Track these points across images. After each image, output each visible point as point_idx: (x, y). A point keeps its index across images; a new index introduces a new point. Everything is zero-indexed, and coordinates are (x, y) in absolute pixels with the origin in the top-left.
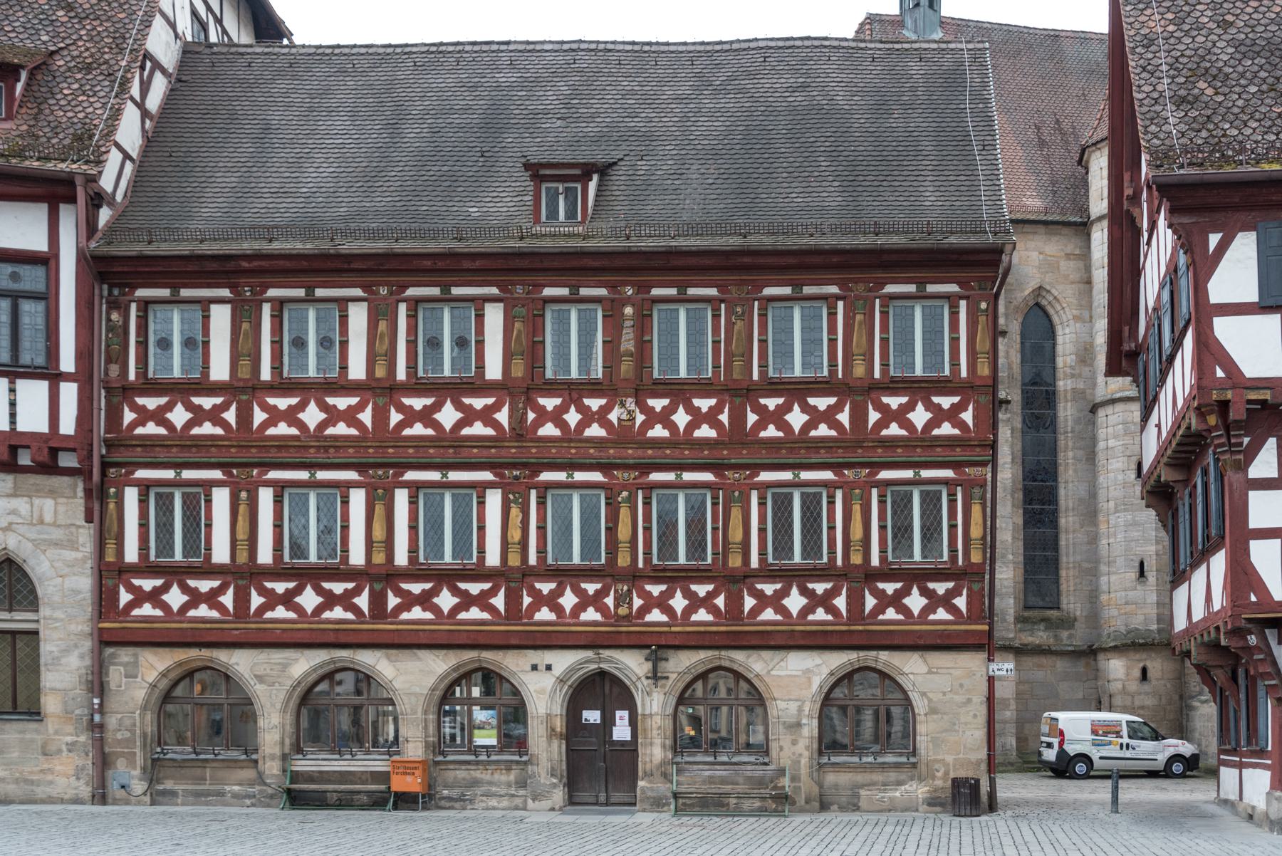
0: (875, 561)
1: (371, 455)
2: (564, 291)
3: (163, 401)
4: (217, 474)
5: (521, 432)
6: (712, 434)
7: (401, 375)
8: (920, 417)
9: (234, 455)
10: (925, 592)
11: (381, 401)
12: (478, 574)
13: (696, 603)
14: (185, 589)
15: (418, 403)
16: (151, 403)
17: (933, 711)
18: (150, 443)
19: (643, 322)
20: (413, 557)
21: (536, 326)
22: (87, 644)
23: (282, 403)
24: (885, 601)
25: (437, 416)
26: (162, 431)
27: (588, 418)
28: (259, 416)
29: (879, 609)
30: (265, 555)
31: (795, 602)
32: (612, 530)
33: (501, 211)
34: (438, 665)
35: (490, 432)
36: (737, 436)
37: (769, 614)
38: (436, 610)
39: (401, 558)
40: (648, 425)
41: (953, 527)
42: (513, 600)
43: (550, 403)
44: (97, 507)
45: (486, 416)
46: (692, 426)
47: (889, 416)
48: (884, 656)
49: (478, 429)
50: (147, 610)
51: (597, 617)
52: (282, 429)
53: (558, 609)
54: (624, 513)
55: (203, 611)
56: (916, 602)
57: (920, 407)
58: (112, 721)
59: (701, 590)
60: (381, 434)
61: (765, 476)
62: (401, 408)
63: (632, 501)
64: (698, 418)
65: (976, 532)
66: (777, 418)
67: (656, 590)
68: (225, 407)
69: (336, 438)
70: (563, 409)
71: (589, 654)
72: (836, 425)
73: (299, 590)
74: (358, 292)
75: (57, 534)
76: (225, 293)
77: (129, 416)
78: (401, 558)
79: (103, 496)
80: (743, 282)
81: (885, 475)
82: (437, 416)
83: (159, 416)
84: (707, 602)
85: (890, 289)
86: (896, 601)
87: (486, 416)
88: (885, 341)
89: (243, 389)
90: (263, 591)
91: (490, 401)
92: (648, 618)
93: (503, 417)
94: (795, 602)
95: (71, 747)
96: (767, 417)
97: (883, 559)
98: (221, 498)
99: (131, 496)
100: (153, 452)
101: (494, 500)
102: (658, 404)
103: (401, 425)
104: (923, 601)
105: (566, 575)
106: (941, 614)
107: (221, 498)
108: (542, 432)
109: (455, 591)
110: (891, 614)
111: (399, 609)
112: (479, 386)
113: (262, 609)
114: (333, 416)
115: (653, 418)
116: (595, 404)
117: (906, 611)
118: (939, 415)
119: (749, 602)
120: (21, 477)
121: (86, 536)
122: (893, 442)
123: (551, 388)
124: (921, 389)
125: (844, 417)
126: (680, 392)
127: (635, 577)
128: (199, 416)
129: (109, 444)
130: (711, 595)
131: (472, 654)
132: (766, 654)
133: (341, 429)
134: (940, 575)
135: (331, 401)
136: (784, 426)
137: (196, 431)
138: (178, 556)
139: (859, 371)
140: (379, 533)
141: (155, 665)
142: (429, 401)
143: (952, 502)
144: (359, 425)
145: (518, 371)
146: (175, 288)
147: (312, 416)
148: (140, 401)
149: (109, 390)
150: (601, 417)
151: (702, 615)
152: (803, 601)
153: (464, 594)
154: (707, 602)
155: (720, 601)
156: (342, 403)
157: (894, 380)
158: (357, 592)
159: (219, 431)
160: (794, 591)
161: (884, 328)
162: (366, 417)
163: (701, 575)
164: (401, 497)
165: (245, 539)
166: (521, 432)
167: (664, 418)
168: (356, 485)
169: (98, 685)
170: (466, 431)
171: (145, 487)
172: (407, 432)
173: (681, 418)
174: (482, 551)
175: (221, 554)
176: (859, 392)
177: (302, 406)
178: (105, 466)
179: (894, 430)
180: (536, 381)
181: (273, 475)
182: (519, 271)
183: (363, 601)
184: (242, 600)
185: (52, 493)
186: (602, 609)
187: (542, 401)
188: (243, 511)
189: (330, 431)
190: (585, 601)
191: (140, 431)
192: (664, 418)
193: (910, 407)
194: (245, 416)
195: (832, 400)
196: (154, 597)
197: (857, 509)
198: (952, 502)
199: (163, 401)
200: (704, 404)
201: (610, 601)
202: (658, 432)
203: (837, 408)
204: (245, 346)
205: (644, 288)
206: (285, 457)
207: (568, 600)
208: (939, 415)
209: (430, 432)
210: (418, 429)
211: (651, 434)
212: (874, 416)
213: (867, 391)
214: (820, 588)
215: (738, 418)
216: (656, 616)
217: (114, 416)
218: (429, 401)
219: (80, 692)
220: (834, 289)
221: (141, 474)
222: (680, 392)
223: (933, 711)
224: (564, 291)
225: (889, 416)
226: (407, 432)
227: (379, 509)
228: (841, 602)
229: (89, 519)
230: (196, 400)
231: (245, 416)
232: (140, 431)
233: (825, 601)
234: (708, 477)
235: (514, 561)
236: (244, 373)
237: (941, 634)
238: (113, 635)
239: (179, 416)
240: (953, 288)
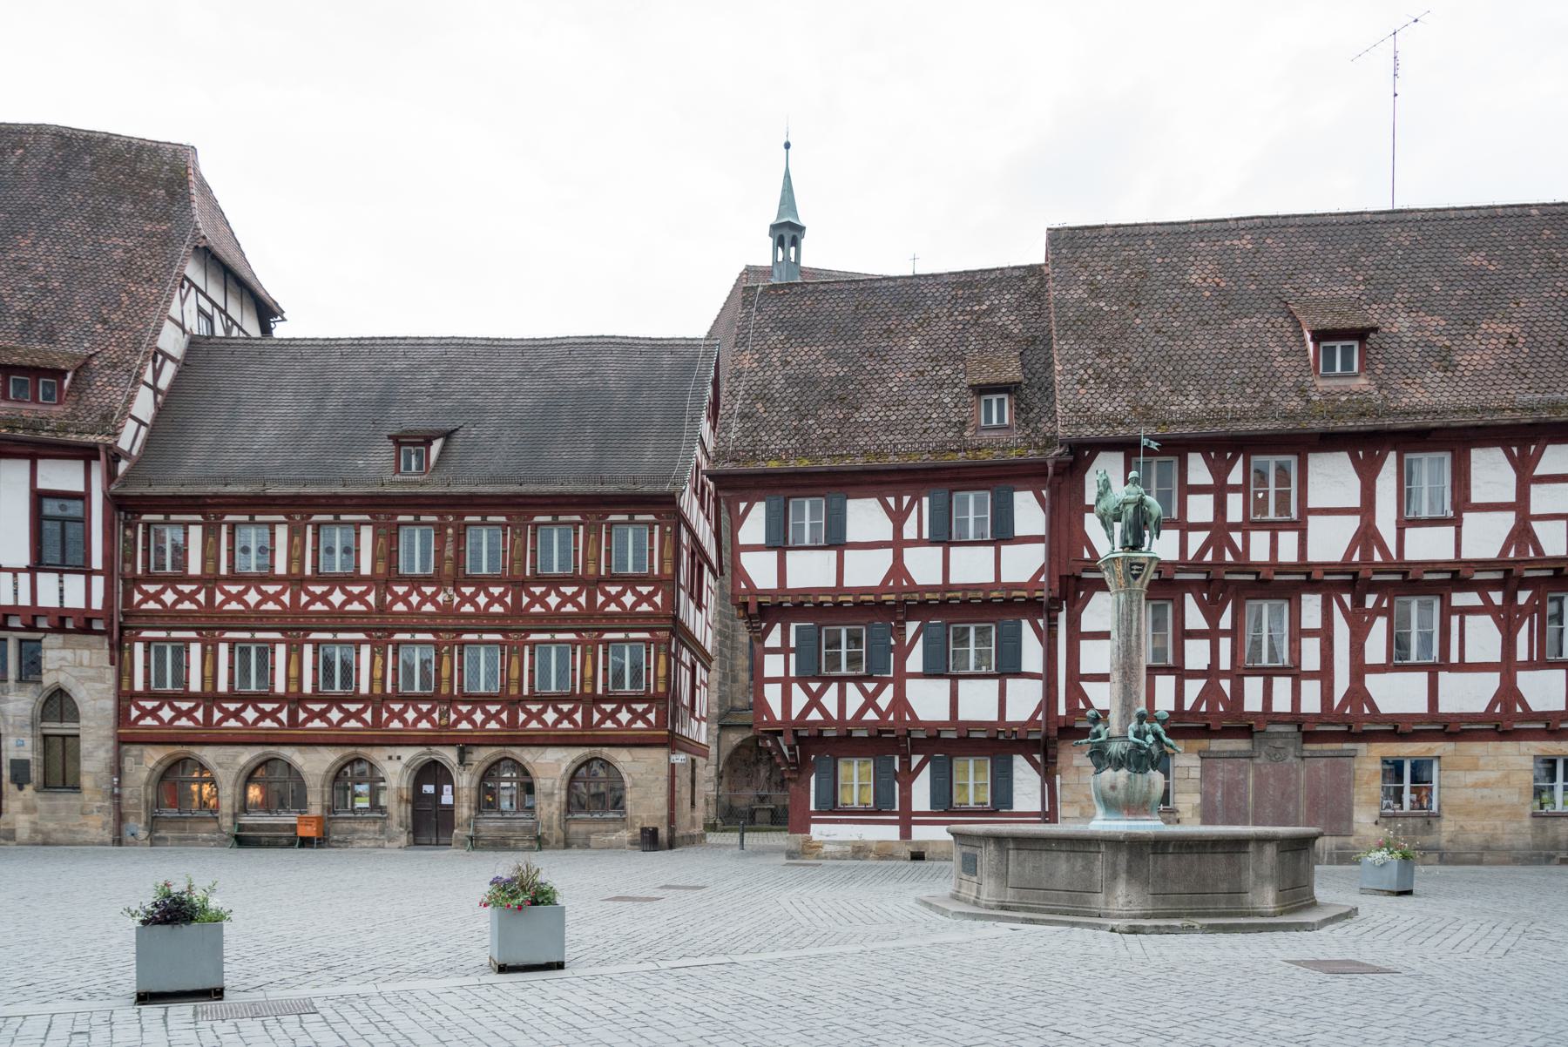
0: (600, 691)
1: (289, 623)
2: (410, 518)
3: (159, 587)
4: (193, 634)
5: (382, 608)
7: (308, 571)
8: (629, 599)
9: (204, 623)
10: (630, 710)
11: (295, 588)
13: (489, 717)
15: (318, 590)
16: (152, 589)
17: (635, 785)
18: (151, 614)
19: (460, 538)
21: (393, 540)
23: (234, 589)
25: (331, 598)
26: (158, 607)
27: (425, 599)
28: (219, 598)
31: (550, 716)
32: (438, 671)
33: (377, 468)
35: (363, 608)
36: (516, 611)
37: (534, 724)
40: (461, 604)
41: (648, 669)
43: (401, 590)
44: (117, 655)
45: (361, 598)
46: (488, 605)
47: (610, 599)
48: (605, 750)
49: (356, 606)
52: (234, 606)
54: (446, 660)
56: (624, 716)
57: (629, 593)
59: (493, 709)
60: (295, 609)
61: (534, 637)
62: (308, 593)
64: (492, 600)
65: (662, 672)
66: (541, 600)
67: (464, 709)
68: (198, 591)
69: (267, 612)
70: (409, 594)
72: (577, 604)
74: (282, 518)
75: (91, 673)
77: (137, 597)
79: (121, 648)
80: (520, 514)
81: (607, 636)
82: (331, 598)
83: (156, 596)
84: (496, 716)
85: (612, 518)
86: (612, 716)
87: (361, 598)
88: (609, 552)
89: (210, 580)
91: (363, 588)
92: (460, 727)
93: (371, 598)
94: (550, 716)
96: (535, 599)
97: (605, 689)
98: (195, 649)
99: (139, 648)
101: (366, 651)
102: (468, 591)
103: (308, 604)
104: (629, 716)
108: (395, 608)
112: (356, 579)
114: (266, 597)
115: (465, 599)
116: (429, 590)
117: (618, 722)
118: (641, 599)
119: (522, 717)
120: (68, 636)
122: (613, 615)
123: (401, 580)
124: (629, 582)
125: (582, 600)
126: (482, 583)
127: (451, 701)
128: (182, 597)
129: (125, 615)
130: (499, 712)
132: (533, 749)
133: (270, 606)
134: (639, 700)
135: (264, 588)
136: (546, 605)
137: (179, 607)
139: (591, 570)
140: (293, 673)
142: (325, 588)
143: (648, 653)
144: (282, 603)
145: (381, 569)
147: (252, 597)
148: (145, 587)
150: (432, 599)
151: (493, 725)
152: (555, 716)
153: (346, 711)
154: (496, 716)
155: (504, 716)
156: (271, 589)
157: (613, 576)
159: (194, 607)
160: (550, 709)
161: (609, 543)
162: (286, 598)
164: (308, 650)
166: (382, 608)
167: (472, 600)
168: (280, 641)
170: (348, 608)
171: (148, 643)
172: (312, 608)
173: (482, 600)
174: (358, 684)
176: (591, 583)
177: (246, 591)
178: (122, 629)
179: (613, 608)
180: (394, 576)
181: (228, 635)
182: (383, 508)
185: (88, 646)
187: (396, 589)
188: (210, 658)
189: (264, 607)
190: (421, 716)
191: (144, 606)
192: (472, 600)
193: (623, 593)
194: (210, 597)
195: (575, 589)
197: (589, 657)
198: (648, 653)
199: (159, 587)
200: (496, 591)
201: (436, 716)
202: (468, 608)
203: (578, 594)
204: (210, 553)
205: (461, 516)
206: (235, 623)
207: (411, 715)
208: (641, 599)
209: (326, 608)
210: (318, 606)
211: (463, 609)
212: (600, 599)
213: (598, 582)
214: (566, 707)
215: (517, 600)
216: (464, 725)
217: (128, 597)
218: (325, 588)
220: (577, 518)
221: (145, 634)
222: (482, 583)
223: (635, 785)
224: (410, 518)
225: (610, 599)
226: (312, 608)
227: (294, 657)
228: (578, 717)
229: (112, 663)
230: (180, 587)
231: (210, 597)
232: (144, 606)
233: (568, 716)
235: (377, 690)
237: (639, 737)
239: (169, 597)
240: (651, 517)
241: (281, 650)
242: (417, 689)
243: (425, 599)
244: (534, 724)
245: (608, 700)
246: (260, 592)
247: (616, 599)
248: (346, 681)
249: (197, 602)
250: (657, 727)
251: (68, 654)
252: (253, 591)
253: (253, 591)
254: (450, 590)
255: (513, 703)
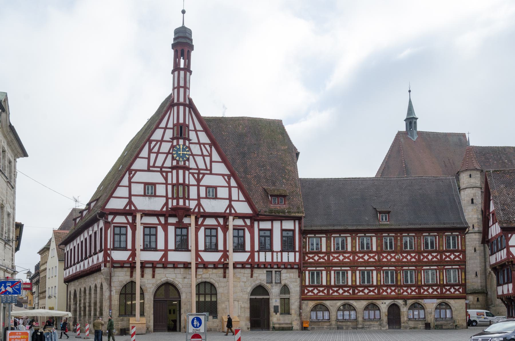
0: (445, 283)
4: (323, 268)
5: (379, 260)
6: (415, 260)
9: (327, 265)
10: (454, 288)
12: (372, 286)
13: (412, 291)
14: (317, 290)
16: (311, 256)
18: (311, 263)
19: (401, 240)
20: (360, 284)
22: (299, 300)
24: (447, 290)
27: (392, 257)
28: (331, 258)
29: (446, 292)
30: (333, 283)
32: (397, 278)
34: (364, 303)
35: (374, 260)
37: (426, 293)
38: (364, 293)
39: (358, 284)
40: (403, 259)
42: (379, 291)
43: (385, 255)
45: (373, 257)
46: (411, 259)
48: (447, 300)
49: (372, 260)
50: (310, 294)
51: (394, 294)
52: (336, 260)
53: (387, 292)
54: (399, 275)
55: (321, 294)
56: (452, 290)
58: (303, 315)
59: (413, 289)
61: (424, 268)
62: (358, 256)
63: (400, 272)
64: (412, 257)
65: (463, 277)
66: (426, 257)
67: (405, 289)
68: (325, 256)
71: (393, 300)
72: (437, 258)
73: (339, 290)
75: (294, 280)
76: (324, 235)
77: (307, 258)
78: (358, 284)
79: (302, 273)
81: (446, 267)
84: (414, 291)
86: (449, 290)
87: (373, 257)
89: (328, 253)
90: (332, 290)
93: (376, 257)
95: (296, 320)
97: (446, 282)
98: (324, 273)
99: (307, 272)
100: (311, 264)
101: (375, 273)
102: (405, 255)
103: (358, 259)
105: (388, 286)
106: (457, 292)
107: (324, 273)
109: (368, 289)
110: (448, 292)
111: (358, 293)
112: (372, 252)
113: (332, 293)
114: (345, 258)
115: (404, 257)
116: (393, 255)
119: (422, 291)
121: (298, 280)
123: (385, 252)
125: (439, 257)
127: (401, 286)
128: (320, 258)
129: (303, 263)
130: (415, 290)
131: (371, 301)
133: (347, 260)
134: (457, 285)
138: (316, 283)
140: (354, 279)
141: (311, 304)
143: (458, 272)
144: (350, 259)
145: (379, 249)
146: (315, 235)
149: (303, 253)
150: (394, 257)
151: (414, 293)
153: (370, 290)
154: (414, 291)
155: (417, 291)
156: (347, 255)
158: (350, 290)
162: (351, 258)
163: (413, 286)
164: (358, 272)
165: (329, 280)
166: (379, 260)
167: (406, 257)
169: (300, 308)
170: (370, 260)
175: (324, 283)
177: (339, 256)
181: (334, 268)
182: (378, 232)
183: (351, 291)
184: (328, 291)
185: (293, 273)
186: (395, 292)
188: (329, 275)
192: (406, 257)
194: (329, 258)
196: (312, 291)
197: (441, 274)
200: (413, 255)
201: (397, 291)
202: (405, 260)
210: (361, 260)
214: (435, 288)
215: (419, 257)
216: (405, 293)
217: (304, 258)
219: (298, 309)
227: (354, 275)
228: (439, 290)
229: (299, 277)
230: (319, 255)
231: (329, 258)
233: (436, 290)
234: (414, 268)
236: (329, 250)
238: (304, 298)
239: (316, 258)
241: (350, 273)
242: (390, 283)
243: (392, 257)
244: (426, 293)
245: (447, 285)
246: (343, 256)
247: (449, 257)
248: (369, 281)
249: (325, 259)
250: (463, 293)
251: (288, 275)
252: (341, 256)
253: (341, 256)
254: (400, 255)
255: (419, 287)
